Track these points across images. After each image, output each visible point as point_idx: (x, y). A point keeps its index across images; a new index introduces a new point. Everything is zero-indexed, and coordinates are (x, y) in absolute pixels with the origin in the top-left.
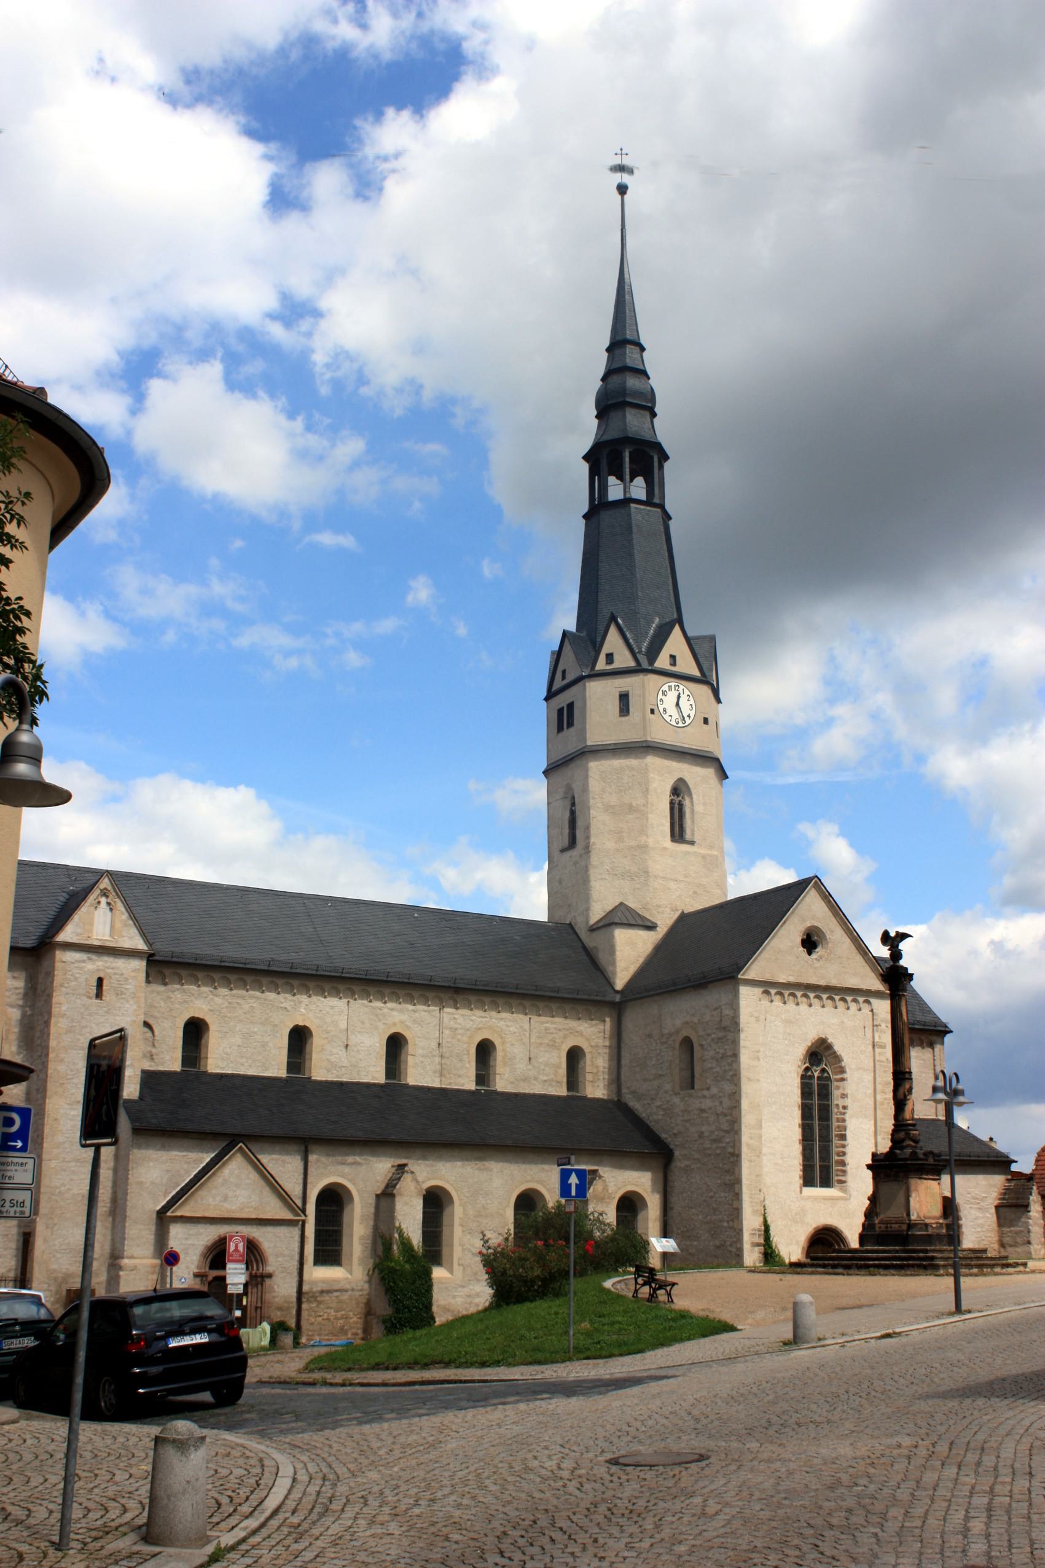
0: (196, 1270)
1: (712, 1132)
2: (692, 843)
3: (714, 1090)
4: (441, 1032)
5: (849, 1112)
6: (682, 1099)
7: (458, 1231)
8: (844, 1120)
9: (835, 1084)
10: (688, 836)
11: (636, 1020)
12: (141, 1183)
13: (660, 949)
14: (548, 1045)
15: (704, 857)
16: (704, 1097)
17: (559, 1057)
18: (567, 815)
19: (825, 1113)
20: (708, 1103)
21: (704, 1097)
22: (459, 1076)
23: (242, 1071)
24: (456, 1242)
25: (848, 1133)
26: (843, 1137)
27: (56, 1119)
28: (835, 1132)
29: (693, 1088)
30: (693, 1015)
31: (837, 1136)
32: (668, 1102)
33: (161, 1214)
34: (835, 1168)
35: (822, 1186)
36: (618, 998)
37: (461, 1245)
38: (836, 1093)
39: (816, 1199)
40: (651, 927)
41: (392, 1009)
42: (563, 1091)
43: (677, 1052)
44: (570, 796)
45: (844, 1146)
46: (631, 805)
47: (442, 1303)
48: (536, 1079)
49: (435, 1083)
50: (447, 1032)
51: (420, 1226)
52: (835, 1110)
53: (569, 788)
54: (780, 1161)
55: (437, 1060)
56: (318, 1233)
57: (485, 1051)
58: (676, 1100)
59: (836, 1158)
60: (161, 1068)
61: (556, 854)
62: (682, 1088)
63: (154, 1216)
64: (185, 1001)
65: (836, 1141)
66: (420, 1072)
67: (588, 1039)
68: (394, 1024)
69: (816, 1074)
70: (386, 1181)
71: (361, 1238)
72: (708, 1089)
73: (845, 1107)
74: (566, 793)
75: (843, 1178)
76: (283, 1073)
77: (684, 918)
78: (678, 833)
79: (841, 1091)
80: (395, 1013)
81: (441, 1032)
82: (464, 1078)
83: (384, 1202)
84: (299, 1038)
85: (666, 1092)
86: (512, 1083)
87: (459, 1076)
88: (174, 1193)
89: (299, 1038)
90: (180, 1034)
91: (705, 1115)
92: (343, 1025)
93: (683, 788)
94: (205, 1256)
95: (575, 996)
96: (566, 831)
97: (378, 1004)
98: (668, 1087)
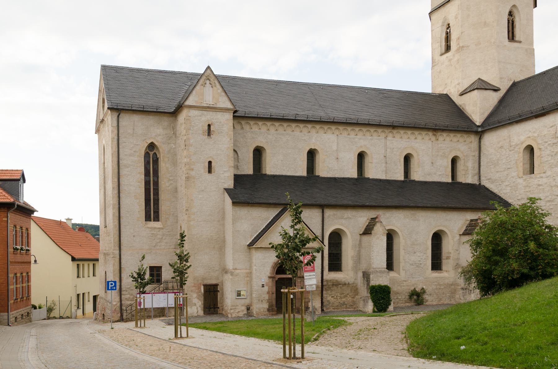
0: (269, 275)
1: (546, 197)
2: (520, 42)
3: (549, 173)
6: (525, 180)
7: (402, 252)
10: (517, 38)
11: (491, 139)
12: (239, 231)
13: (502, 101)
15: (526, 50)
16: (542, 177)
17: (448, 162)
18: (444, 35)
20: (545, 180)
21: (542, 177)
22: (396, 173)
23: (284, 173)
24: (401, 258)
27: (192, 200)
29: (533, 173)
30: (534, 132)
32: (514, 182)
33: (251, 245)
36: (480, 129)
37: (404, 260)
40: (496, 90)
41: (360, 139)
42: (450, 180)
43: (521, 155)
44: (446, 24)
46: (485, 23)
47: (395, 289)
48: (435, 174)
49: (383, 177)
50: (388, 150)
51: (385, 250)
53: (445, 19)
55: (384, 165)
56: (330, 255)
58: (520, 181)
60: (243, 173)
61: (437, 57)
62: (524, 174)
63: (246, 247)
64: (253, 138)
66: (373, 171)
67: (462, 153)
68: (361, 147)
70: (365, 227)
71: (353, 257)
72: (544, 173)
74: (443, 22)
76: (304, 174)
77: (514, 84)
78: (512, 37)
83: (366, 238)
84: (312, 154)
85: (513, 177)
87: (396, 173)
88: (255, 235)
89: (312, 154)
90: (251, 155)
91: (541, 187)
92: (335, 148)
93: (515, 11)
94: (273, 268)
95: (456, 129)
96: (444, 43)
97: (352, 135)
98: (514, 174)
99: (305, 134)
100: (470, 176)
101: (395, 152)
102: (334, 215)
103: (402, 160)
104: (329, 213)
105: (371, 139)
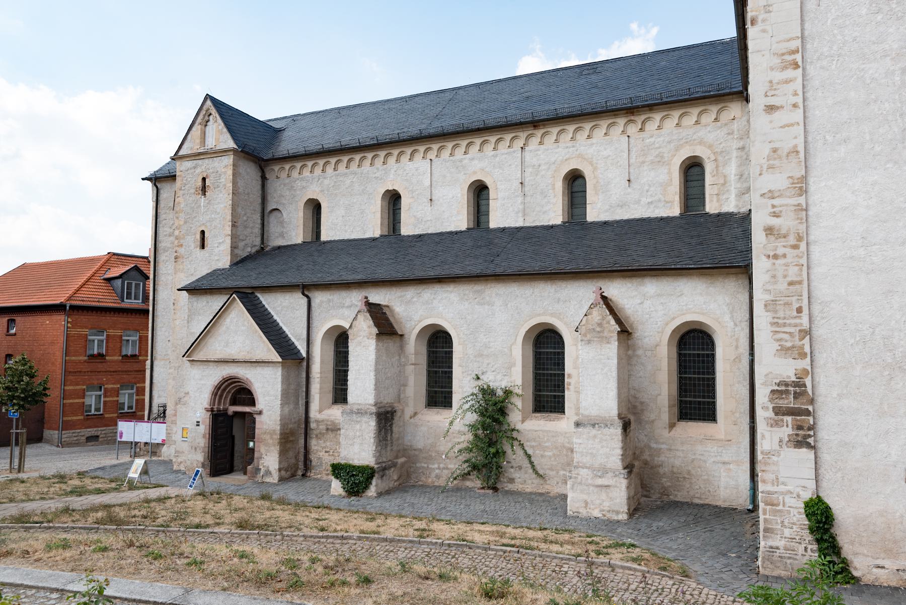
4: (523, 171)
14: (652, 162)
22: (545, 212)
41: (473, 159)
49: (520, 224)
50: (529, 170)
54: (862, 252)
55: (520, 200)
57: (575, 182)
60: (290, 243)
68: (475, 173)
80: (476, 162)
81: (523, 171)
82: (552, 212)
86: (606, 211)
87: (545, 212)
92: (427, 183)
99: (378, 169)
100: (733, 196)
101: (543, 173)
102: (329, 301)
103: (559, 185)
104: (320, 298)
105: (495, 156)
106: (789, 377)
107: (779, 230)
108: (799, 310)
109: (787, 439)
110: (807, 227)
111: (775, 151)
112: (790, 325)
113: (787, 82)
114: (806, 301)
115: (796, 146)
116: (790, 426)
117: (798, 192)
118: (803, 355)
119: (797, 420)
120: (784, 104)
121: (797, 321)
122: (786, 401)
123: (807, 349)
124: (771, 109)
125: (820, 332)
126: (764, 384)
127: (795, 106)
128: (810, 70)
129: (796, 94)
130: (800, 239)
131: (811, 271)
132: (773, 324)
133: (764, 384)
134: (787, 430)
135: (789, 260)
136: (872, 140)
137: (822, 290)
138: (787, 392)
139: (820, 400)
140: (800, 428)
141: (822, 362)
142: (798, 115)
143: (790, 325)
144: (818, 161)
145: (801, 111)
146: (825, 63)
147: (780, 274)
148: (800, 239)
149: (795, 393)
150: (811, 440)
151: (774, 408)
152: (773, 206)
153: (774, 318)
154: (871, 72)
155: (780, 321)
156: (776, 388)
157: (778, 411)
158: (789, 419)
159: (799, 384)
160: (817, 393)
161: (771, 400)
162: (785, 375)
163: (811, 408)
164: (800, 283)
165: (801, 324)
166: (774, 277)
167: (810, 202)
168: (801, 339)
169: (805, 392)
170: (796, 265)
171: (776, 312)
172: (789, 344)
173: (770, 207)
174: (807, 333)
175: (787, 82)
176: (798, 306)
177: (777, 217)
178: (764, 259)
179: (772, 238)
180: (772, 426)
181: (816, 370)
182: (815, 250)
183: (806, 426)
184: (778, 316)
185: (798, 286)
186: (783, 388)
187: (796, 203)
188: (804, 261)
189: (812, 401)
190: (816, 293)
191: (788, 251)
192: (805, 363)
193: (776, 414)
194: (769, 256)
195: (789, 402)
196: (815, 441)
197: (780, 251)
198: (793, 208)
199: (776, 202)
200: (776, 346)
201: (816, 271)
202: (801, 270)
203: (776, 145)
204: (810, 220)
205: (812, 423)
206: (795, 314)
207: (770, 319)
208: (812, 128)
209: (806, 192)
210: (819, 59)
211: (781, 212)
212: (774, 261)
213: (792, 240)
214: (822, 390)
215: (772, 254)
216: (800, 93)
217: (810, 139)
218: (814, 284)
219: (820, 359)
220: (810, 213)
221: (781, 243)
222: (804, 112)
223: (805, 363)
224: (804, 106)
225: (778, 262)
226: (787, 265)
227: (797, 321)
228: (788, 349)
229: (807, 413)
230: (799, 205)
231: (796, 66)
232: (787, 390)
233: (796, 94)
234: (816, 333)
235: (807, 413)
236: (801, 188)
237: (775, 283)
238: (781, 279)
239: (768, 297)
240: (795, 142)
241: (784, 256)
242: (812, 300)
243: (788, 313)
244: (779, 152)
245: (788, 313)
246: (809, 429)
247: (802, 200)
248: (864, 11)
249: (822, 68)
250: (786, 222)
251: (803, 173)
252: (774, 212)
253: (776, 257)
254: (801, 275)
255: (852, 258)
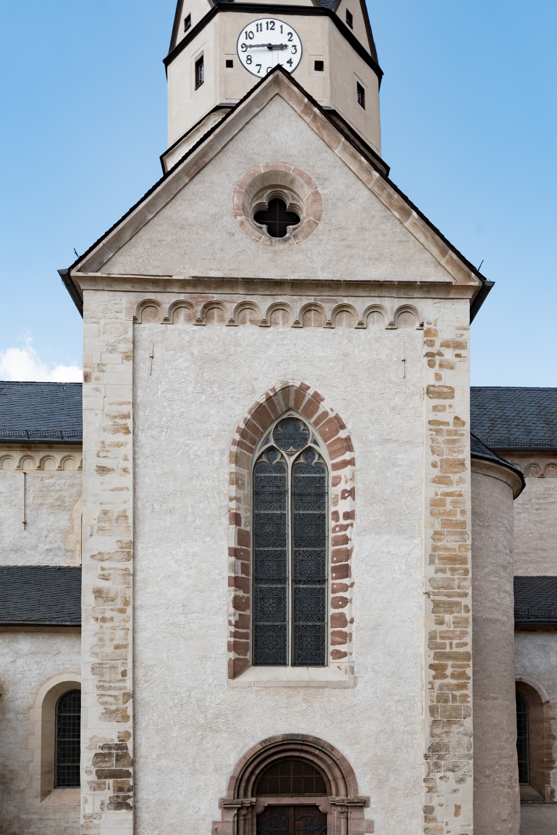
5: (357, 522)
8: (346, 540)
9: (332, 474)
19: (312, 530)
25: (353, 563)
26: (345, 572)
28: (330, 565)
31: (334, 569)
34: (331, 630)
35: (294, 664)
38: (333, 491)
39: (266, 687)
45: (345, 588)
52: (331, 524)
59: (331, 611)
65: (331, 581)
69: (290, 461)
73: (349, 515)
75: (342, 648)
79: (343, 486)
106: (112, 740)
107: (107, 593)
108: (124, 674)
109: (108, 802)
110: (134, 592)
111: (105, 513)
112: (115, 688)
113: (119, 445)
114: (130, 665)
115: (125, 511)
116: (112, 788)
117: (126, 556)
118: (125, 718)
119: (118, 782)
120: (115, 467)
121: (122, 684)
122: (109, 764)
123: (130, 712)
124: (102, 470)
125: (143, 695)
126: (89, 748)
127: (125, 470)
128: (142, 437)
129: (126, 459)
130: (126, 603)
131: (137, 636)
132: (99, 687)
133: (89, 748)
134: (108, 794)
135: (116, 623)
136: (193, 513)
137: (146, 655)
138: (110, 755)
139: (141, 761)
140: (120, 789)
141: (144, 724)
142: (128, 480)
143: (115, 688)
144: (146, 527)
145: (131, 476)
146: (155, 433)
147: (107, 637)
148: (126, 603)
149: (117, 755)
150: (130, 801)
151: (97, 771)
152: (103, 569)
153: (100, 681)
154: (195, 448)
155: (106, 685)
156: (100, 751)
157: (101, 774)
158: (111, 781)
159: (121, 747)
160: (138, 755)
161: (95, 764)
162: (108, 738)
163: (131, 770)
164: (125, 646)
165: (125, 688)
166: (101, 640)
167: (138, 567)
168: (125, 702)
169: (127, 754)
170: (123, 629)
171: (102, 675)
172: (113, 708)
173: (99, 569)
174: (132, 696)
175: (119, 445)
176: (123, 669)
177: (107, 580)
178: (93, 621)
179: (101, 601)
180: (94, 790)
181: (139, 733)
182: (142, 616)
183: (126, 787)
184: (104, 679)
185: (123, 650)
186: (106, 751)
187: (124, 567)
188: (129, 625)
189: (133, 763)
190: (141, 657)
191: (115, 614)
192: (128, 726)
193: (99, 777)
194: (97, 619)
195: (112, 765)
196: (135, 802)
197: (108, 614)
198: (121, 572)
199: (106, 564)
200: (101, 709)
201: (142, 636)
202: (127, 634)
203: (107, 507)
204: (137, 585)
205: (131, 783)
206: (120, 677)
207: (96, 683)
208: (141, 494)
209: (134, 557)
210: (149, 428)
211: (110, 575)
212: (102, 624)
213: (119, 604)
214: (143, 751)
215: (100, 616)
216: (130, 458)
217: (139, 505)
218: (139, 648)
219: (143, 721)
220: (138, 578)
221: (108, 606)
222: (134, 478)
223: (128, 726)
224: (134, 473)
225: (106, 625)
226: (114, 628)
227: (122, 684)
228: (113, 712)
229: (127, 774)
230: (126, 569)
231: (127, 431)
232: (110, 753)
233: (126, 459)
234: (139, 696)
235: (127, 774)
236: (128, 553)
237: (103, 646)
238: (108, 642)
239: (95, 660)
240: (124, 506)
241: (112, 619)
242: (137, 664)
243: (113, 676)
244: (109, 515)
245: (113, 676)
246: (129, 790)
247: (129, 565)
248: (190, 389)
249: (153, 437)
250: (115, 586)
251: (131, 538)
252: (103, 575)
253: (104, 620)
254: (126, 639)
255: (173, 624)
